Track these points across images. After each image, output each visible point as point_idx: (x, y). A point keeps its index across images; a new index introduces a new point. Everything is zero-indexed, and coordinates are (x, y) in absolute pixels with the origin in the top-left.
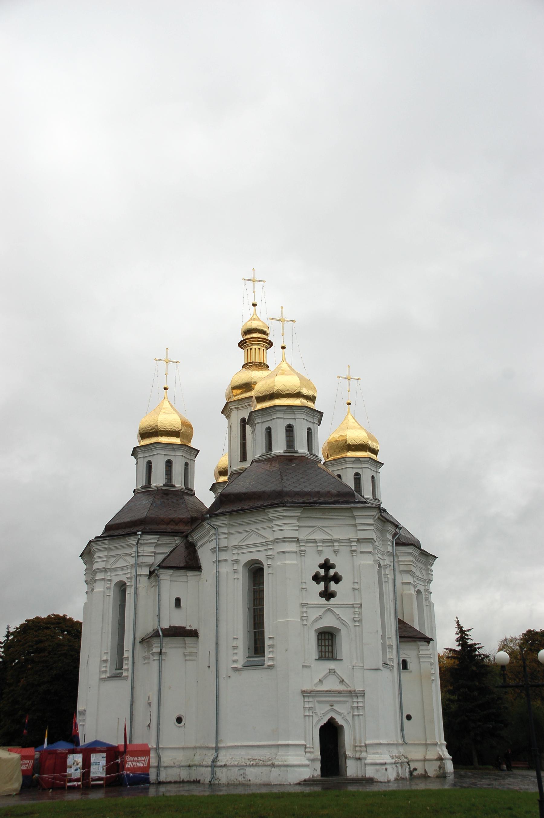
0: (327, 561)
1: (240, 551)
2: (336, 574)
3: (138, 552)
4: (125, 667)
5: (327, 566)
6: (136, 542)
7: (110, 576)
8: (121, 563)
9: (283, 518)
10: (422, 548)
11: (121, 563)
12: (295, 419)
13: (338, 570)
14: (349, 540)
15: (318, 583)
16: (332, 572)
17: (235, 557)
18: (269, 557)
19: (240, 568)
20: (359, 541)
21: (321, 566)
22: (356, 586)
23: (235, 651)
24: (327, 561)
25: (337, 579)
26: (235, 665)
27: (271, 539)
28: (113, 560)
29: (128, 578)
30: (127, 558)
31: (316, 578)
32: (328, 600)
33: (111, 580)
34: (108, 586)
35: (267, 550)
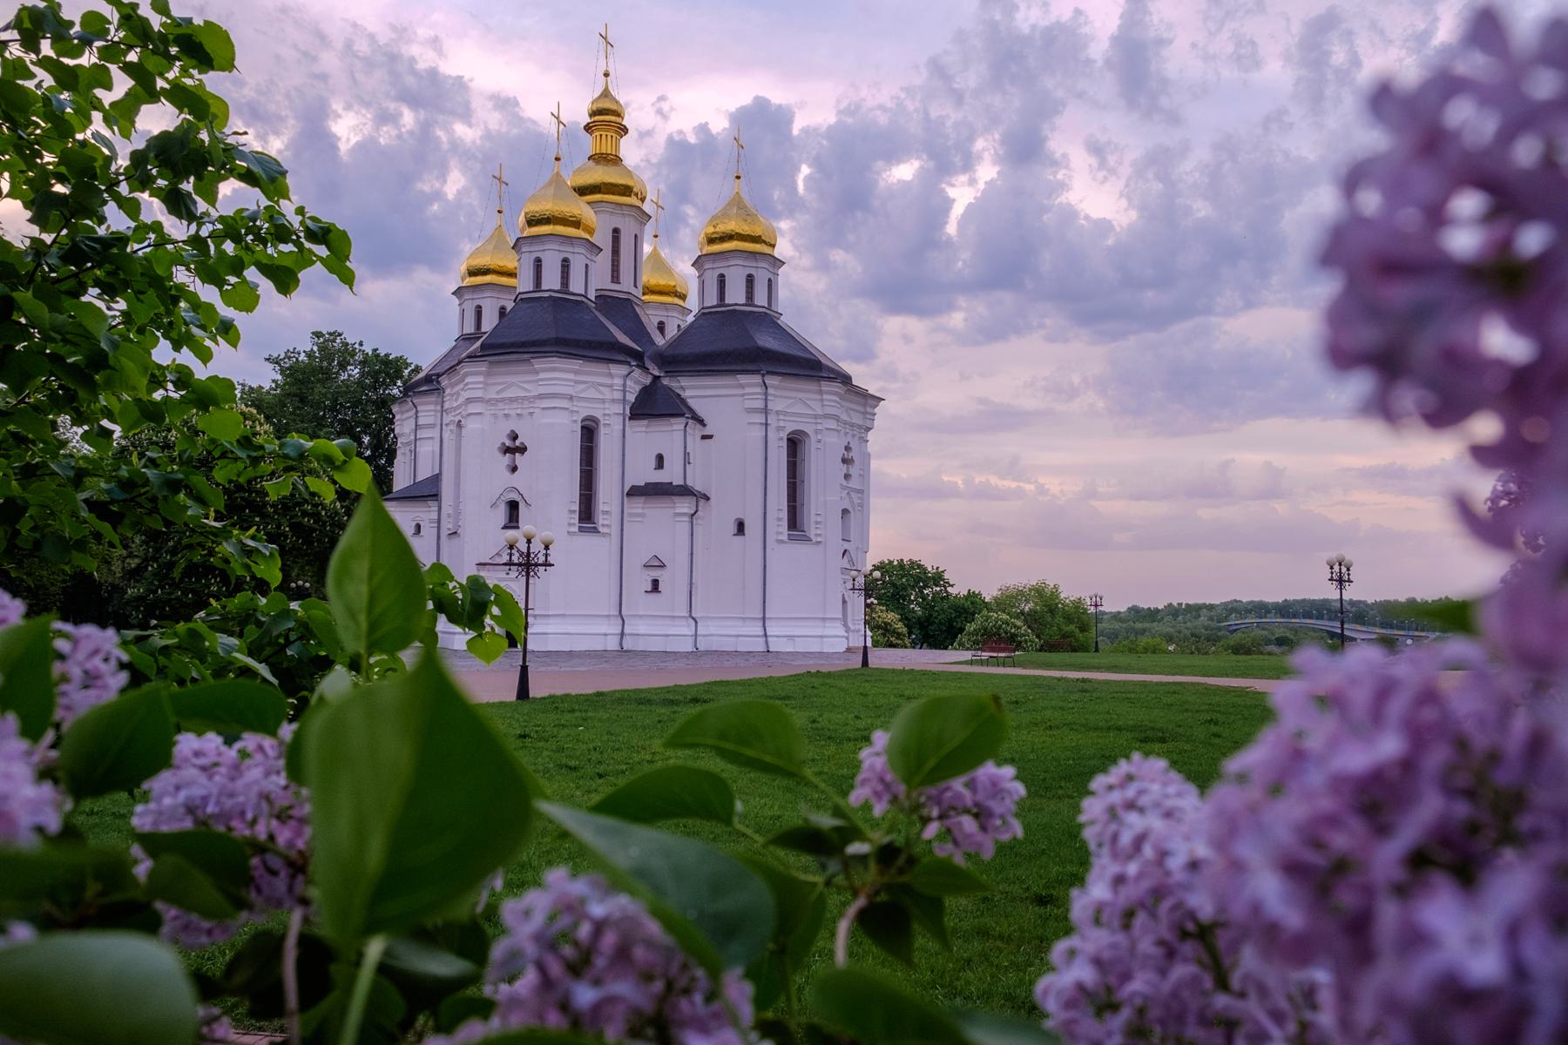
1: (786, 418)
3: (624, 385)
4: (601, 522)
6: (626, 373)
8: (592, 394)
11: (592, 394)
12: (757, 267)
13: (853, 454)
14: (860, 427)
18: (817, 432)
19: (784, 435)
22: (862, 473)
23: (780, 523)
26: (780, 537)
27: (820, 412)
28: (583, 386)
29: (605, 415)
30: (605, 390)
34: (575, 418)
35: (816, 423)
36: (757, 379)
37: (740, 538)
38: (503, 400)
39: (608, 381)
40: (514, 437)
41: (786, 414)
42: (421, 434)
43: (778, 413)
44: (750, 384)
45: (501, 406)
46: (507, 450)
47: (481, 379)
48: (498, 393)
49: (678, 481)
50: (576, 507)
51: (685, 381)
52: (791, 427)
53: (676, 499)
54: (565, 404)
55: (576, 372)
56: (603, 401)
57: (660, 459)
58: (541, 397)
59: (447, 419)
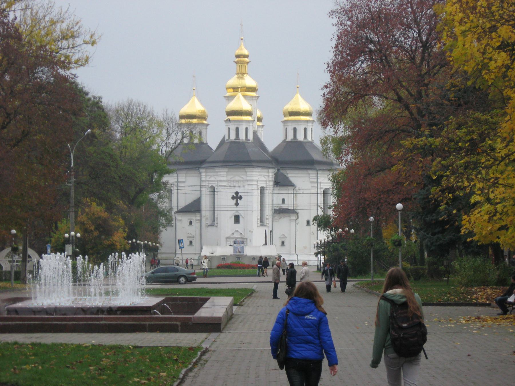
11: (263, 179)
17: (322, 187)
19: (322, 190)
30: (266, 177)
36: (315, 172)
37: (308, 227)
38: (233, 181)
39: (268, 174)
40: (237, 193)
41: (323, 183)
42: (180, 184)
43: (321, 183)
44: (312, 174)
45: (232, 183)
46: (233, 198)
47: (225, 173)
48: (231, 178)
49: (290, 208)
50: (259, 218)
51: (288, 172)
52: (325, 187)
53: (291, 214)
54: (255, 183)
55: (259, 172)
56: (266, 181)
57: (283, 201)
58: (247, 181)
59: (204, 184)
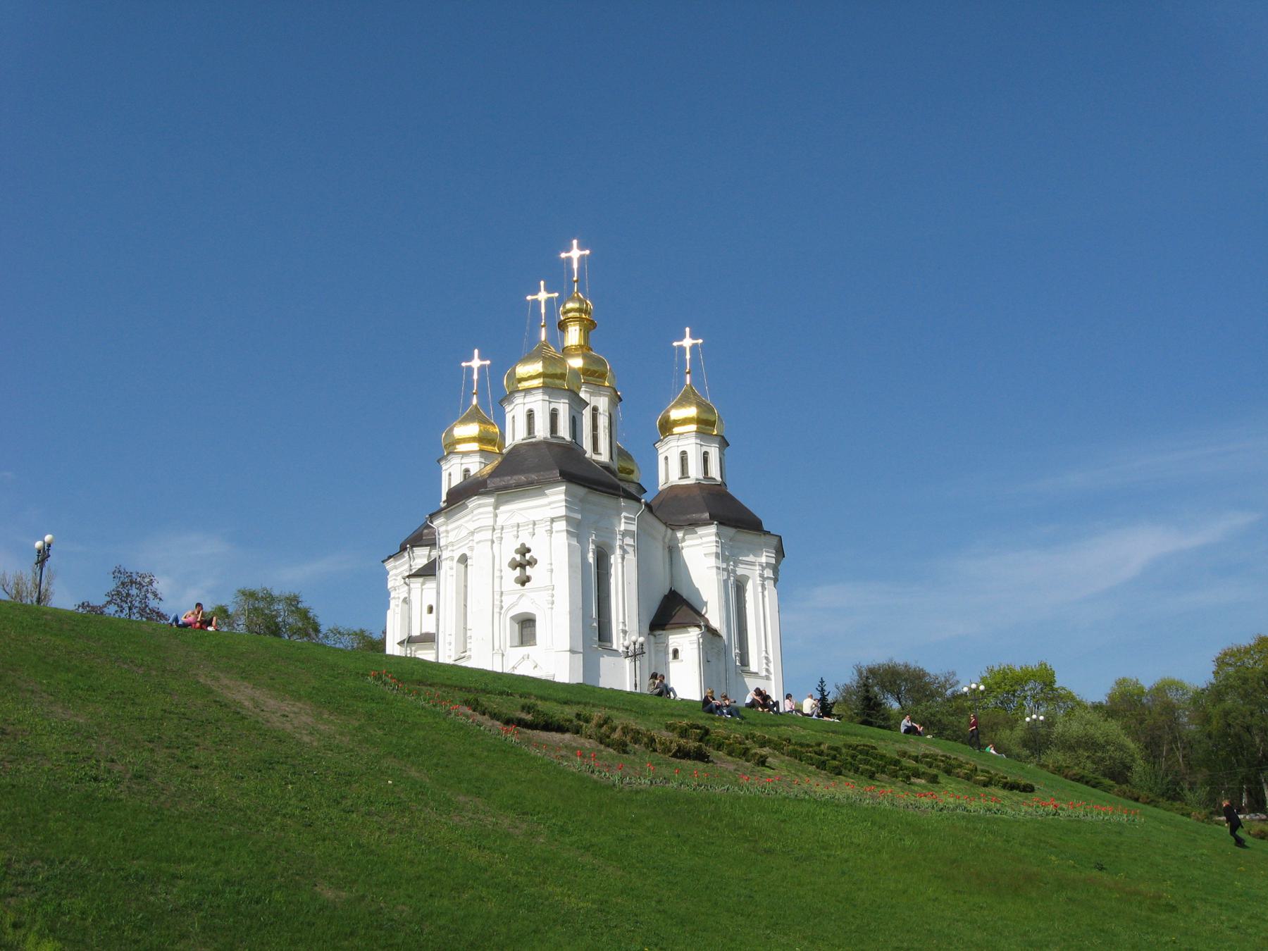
0: (523, 545)
2: (531, 557)
5: (524, 550)
7: (399, 593)
9: (480, 506)
10: (765, 529)
15: (515, 568)
16: (528, 556)
20: (553, 520)
21: (517, 551)
22: (549, 567)
24: (523, 545)
25: (532, 563)
31: (515, 565)
32: (523, 584)
33: (399, 598)
34: (397, 603)
